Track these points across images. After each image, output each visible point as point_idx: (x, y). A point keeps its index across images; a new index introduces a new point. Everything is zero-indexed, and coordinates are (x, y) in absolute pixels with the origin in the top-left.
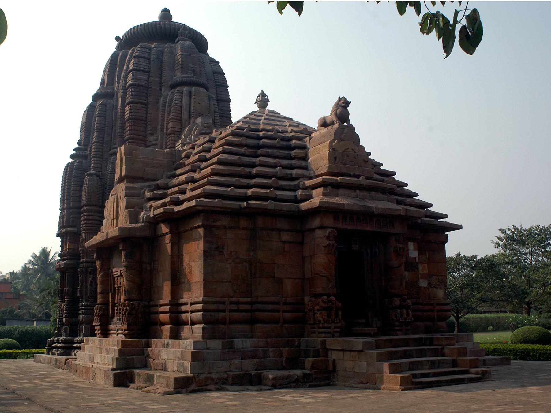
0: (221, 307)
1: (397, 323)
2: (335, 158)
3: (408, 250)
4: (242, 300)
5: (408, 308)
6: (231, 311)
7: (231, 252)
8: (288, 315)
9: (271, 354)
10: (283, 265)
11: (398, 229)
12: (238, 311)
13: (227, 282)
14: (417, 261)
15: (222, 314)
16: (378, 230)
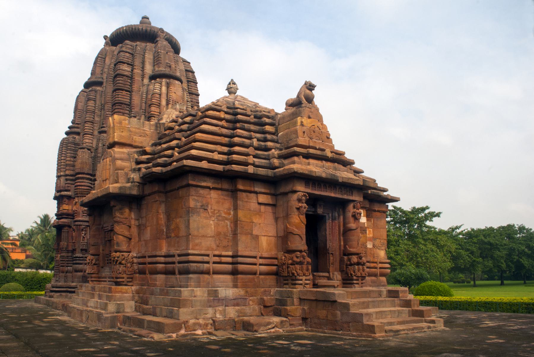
0: (206, 259)
1: (355, 278)
4: (224, 253)
5: (364, 264)
6: (214, 263)
7: (215, 210)
8: (264, 268)
9: (251, 303)
10: (260, 224)
13: (210, 237)
14: (366, 226)
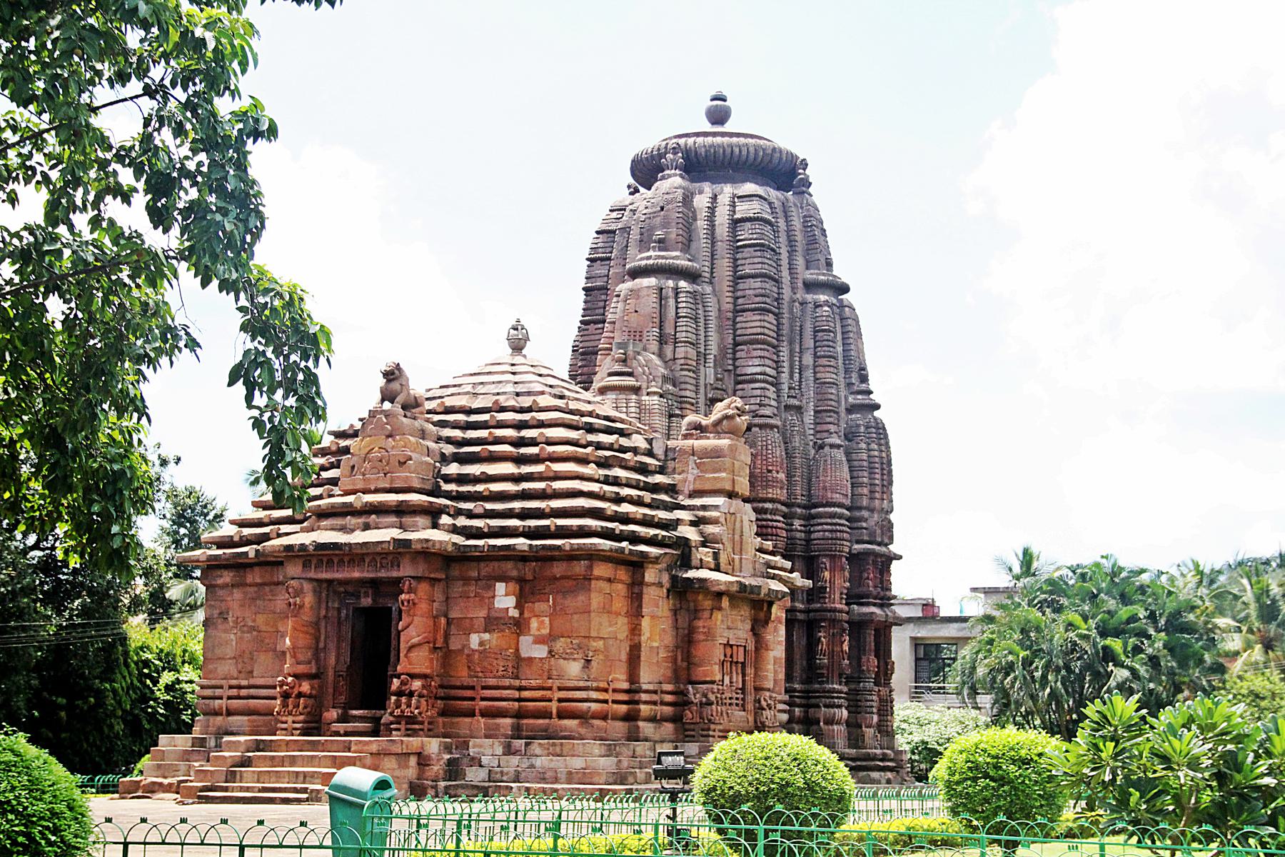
0: (218, 692)
1: (392, 719)
2: (353, 467)
3: (494, 597)
5: (411, 694)
6: (229, 698)
11: (406, 570)
12: (239, 697)
15: (218, 702)
16: (372, 575)
